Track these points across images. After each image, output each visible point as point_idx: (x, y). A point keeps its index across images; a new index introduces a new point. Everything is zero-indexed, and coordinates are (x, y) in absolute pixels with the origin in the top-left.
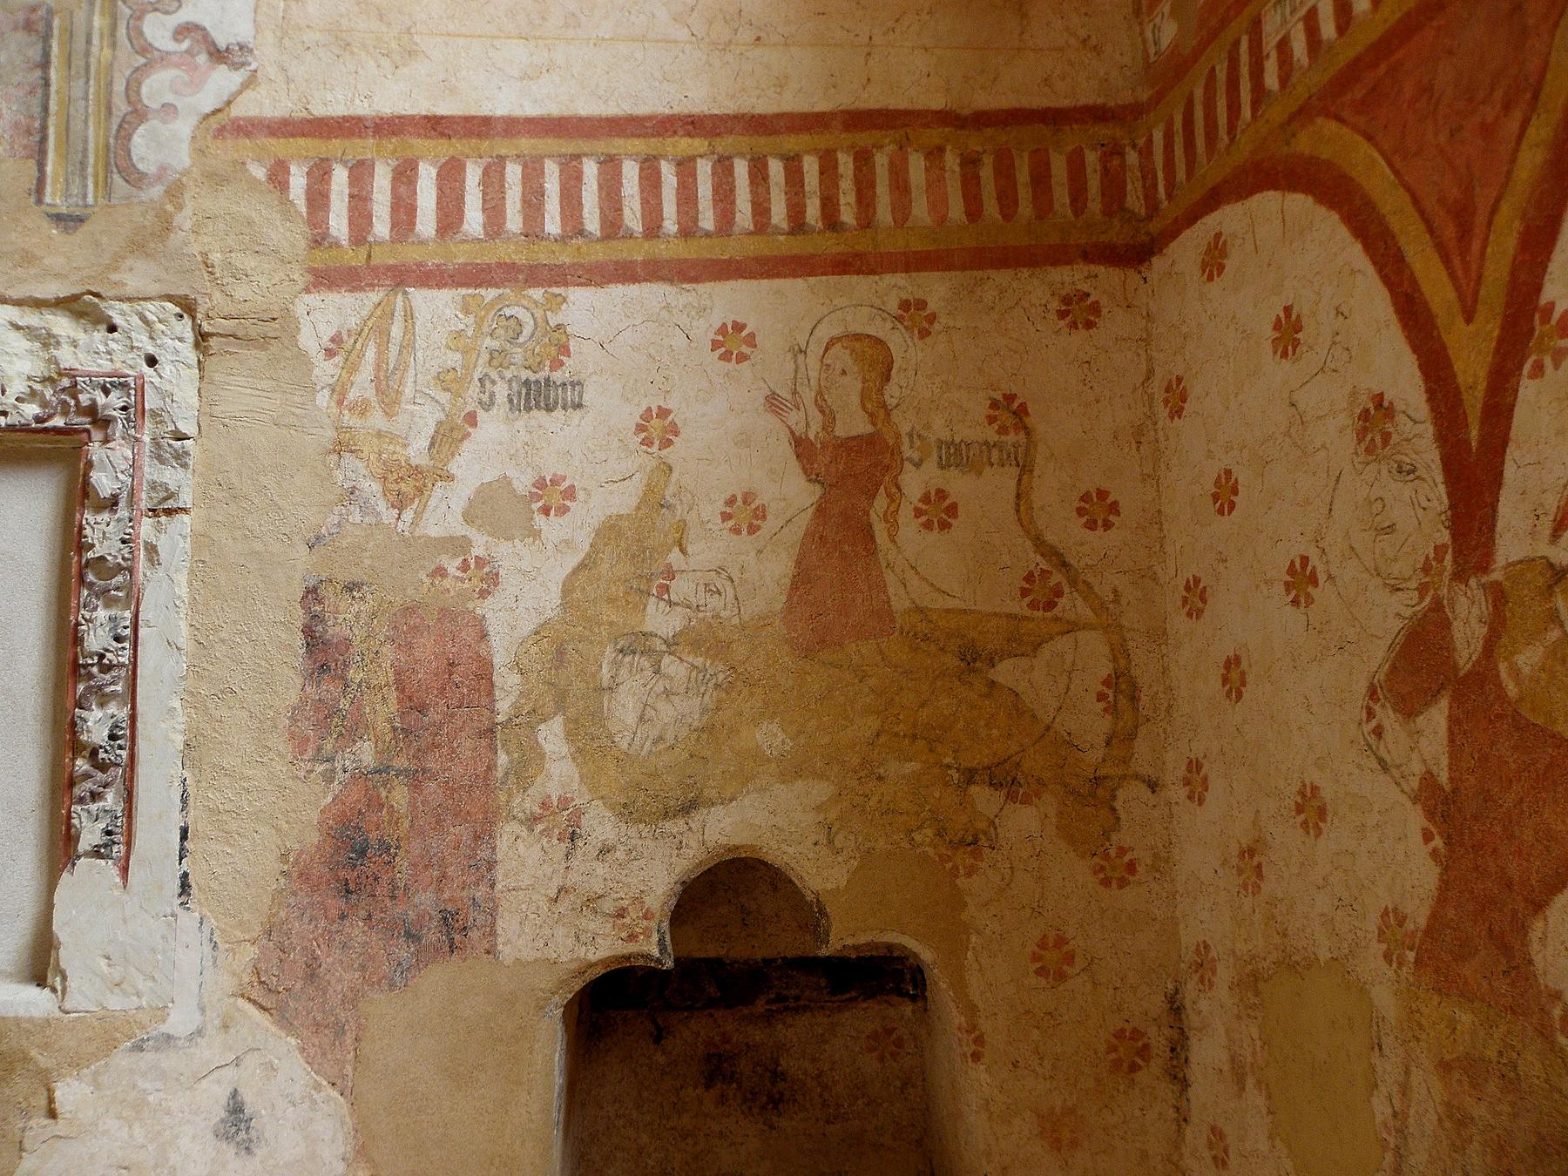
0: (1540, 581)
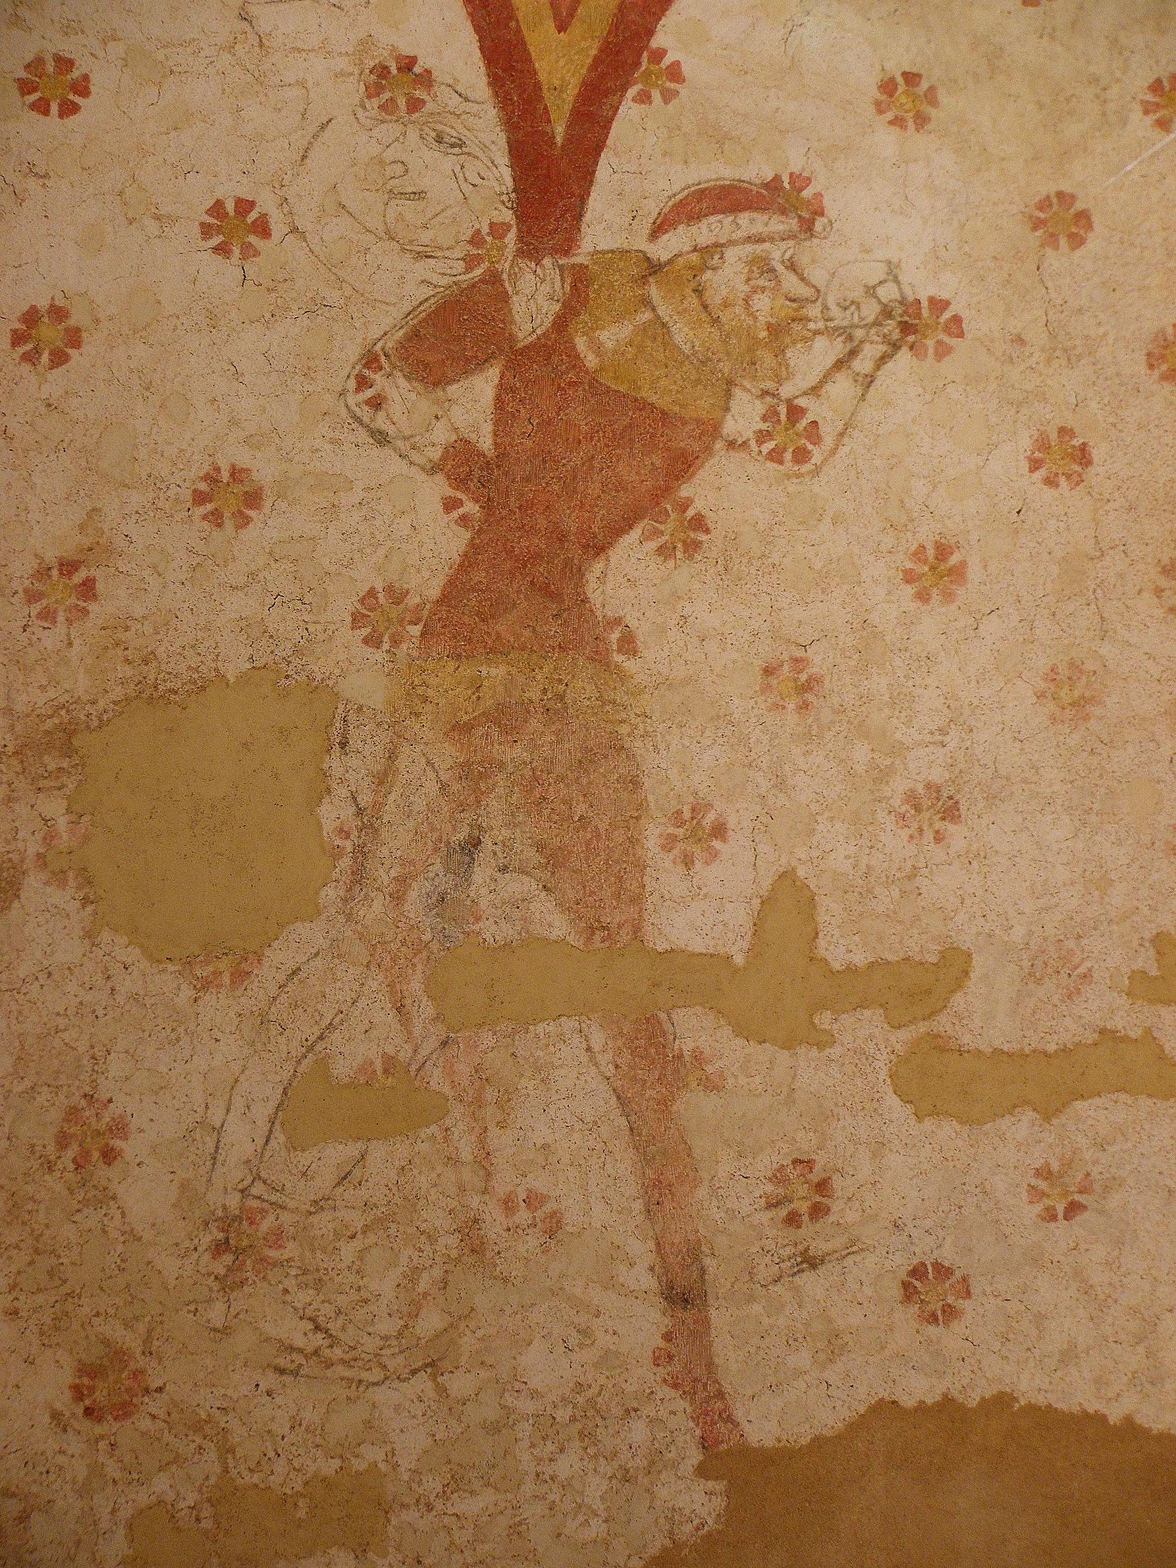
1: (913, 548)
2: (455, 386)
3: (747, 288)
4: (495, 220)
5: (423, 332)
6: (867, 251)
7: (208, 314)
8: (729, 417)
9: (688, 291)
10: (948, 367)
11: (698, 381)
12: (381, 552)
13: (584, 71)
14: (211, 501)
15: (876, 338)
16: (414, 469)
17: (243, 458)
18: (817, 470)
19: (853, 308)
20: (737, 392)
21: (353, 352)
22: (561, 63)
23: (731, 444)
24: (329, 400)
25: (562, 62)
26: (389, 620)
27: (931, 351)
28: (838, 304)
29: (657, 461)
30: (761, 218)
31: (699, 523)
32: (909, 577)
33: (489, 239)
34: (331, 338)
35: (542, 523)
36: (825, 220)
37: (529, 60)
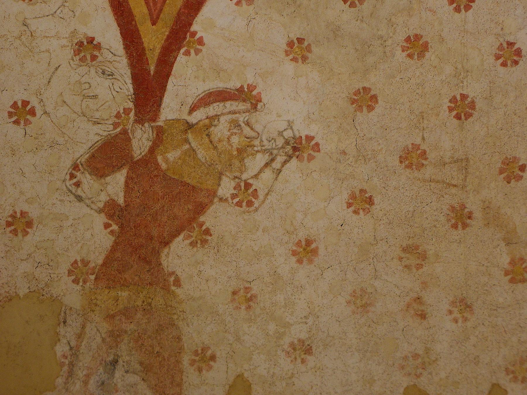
0: (182, 128)
1: (296, 241)
2: (109, 177)
3: (229, 133)
4: (126, 107)
5: (96, 155)
6: (280, 116)
7: (11, 149)
8: (220, 188)
9: (204, 136)
10: (313, 165)
11: (208, 173)
12: (80, 245)
13: (163, 42)
14: (13, 225)
15: (282, 154)
16: (93, 211)
17: (26, 208)
18: (257, 210)
19: (273, 141)
20: (224, 177)
21: (68, 164)
22: (153, 39)
23: (221, 199)
24: (59, 184)
25: (153, 39)
26: (82, 273)
27: (306, 158)
28: (267, 139)
29: (190, 207)
30: (235, 103)
31: (207, 232)
32: (294, 253)
33: (123, 115)
34: (60, 158)
35: (144, 233)
36: (262, 104)
37: (140, 38)
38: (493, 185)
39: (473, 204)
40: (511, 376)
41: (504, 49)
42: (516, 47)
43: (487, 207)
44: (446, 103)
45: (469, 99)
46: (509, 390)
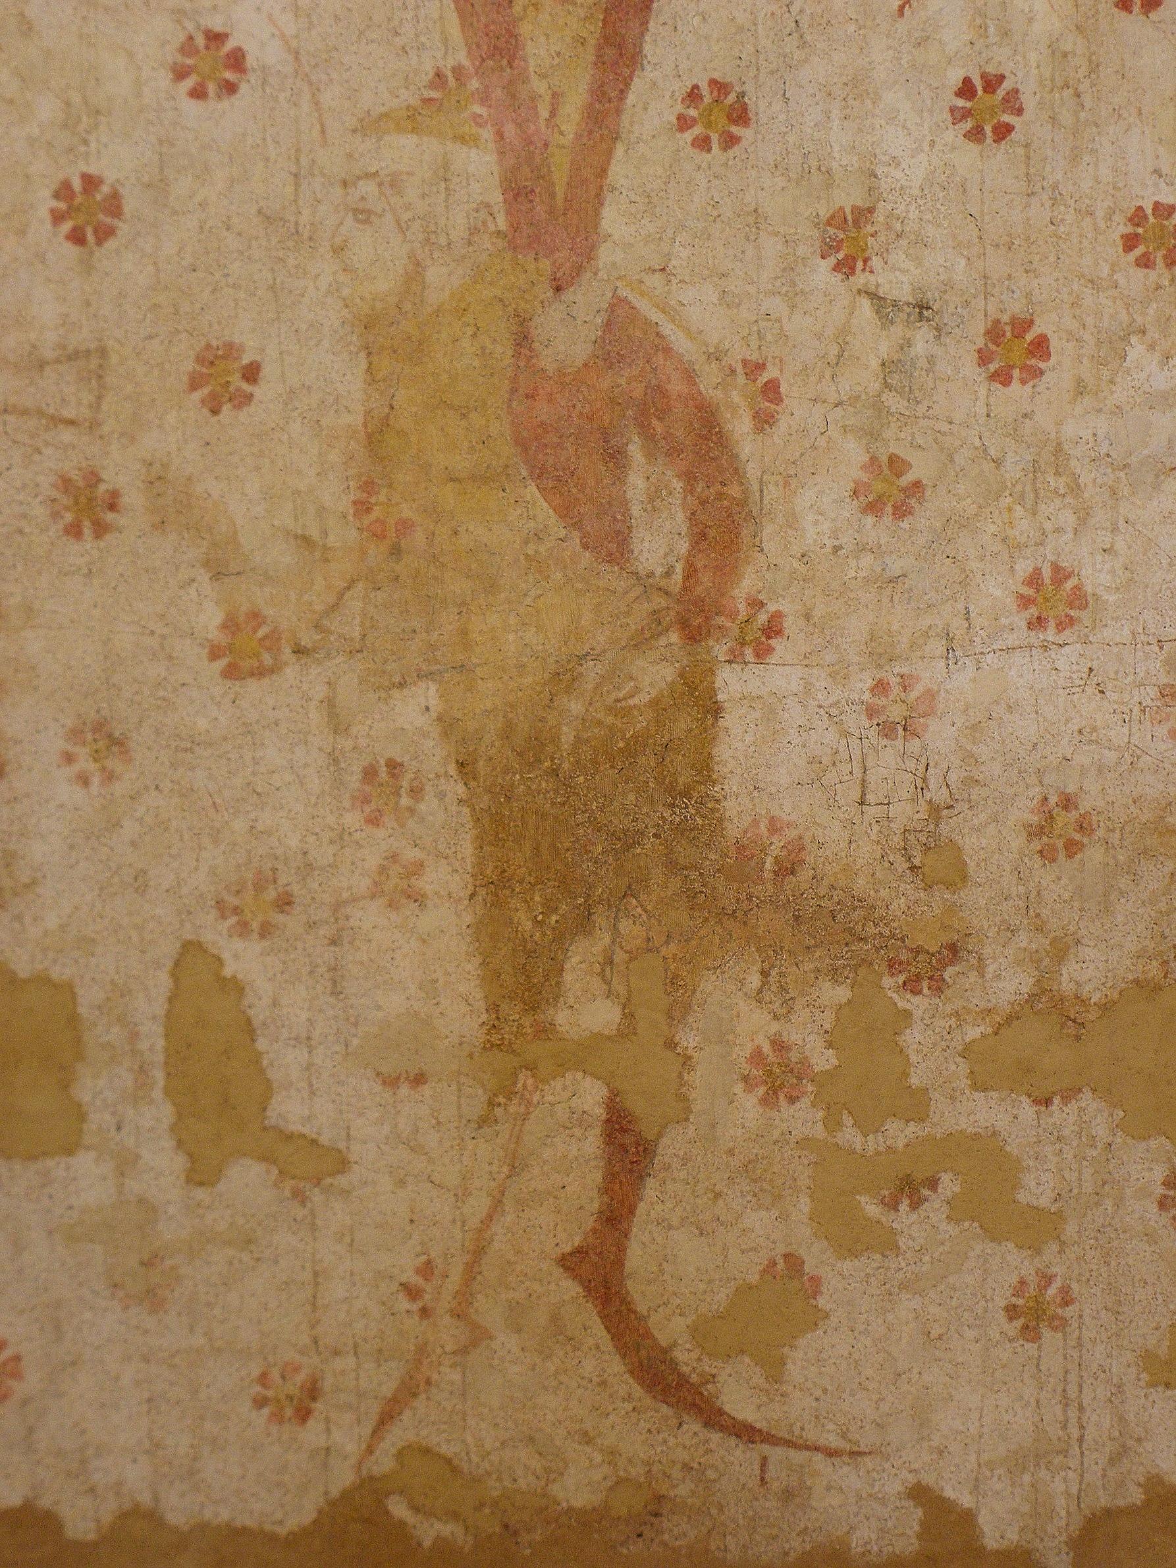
38: (171, 418)
39: (121, 472)
40: (233, 920)
41: (198, 51)
42: (230, 45)
43: (156, 479)
44: (45, 202)
45: (105, 189)
46: (226, 956)
